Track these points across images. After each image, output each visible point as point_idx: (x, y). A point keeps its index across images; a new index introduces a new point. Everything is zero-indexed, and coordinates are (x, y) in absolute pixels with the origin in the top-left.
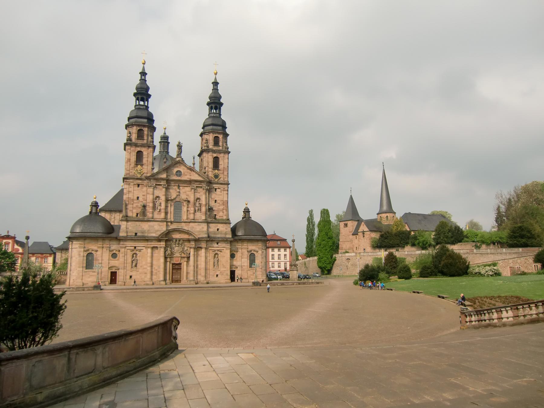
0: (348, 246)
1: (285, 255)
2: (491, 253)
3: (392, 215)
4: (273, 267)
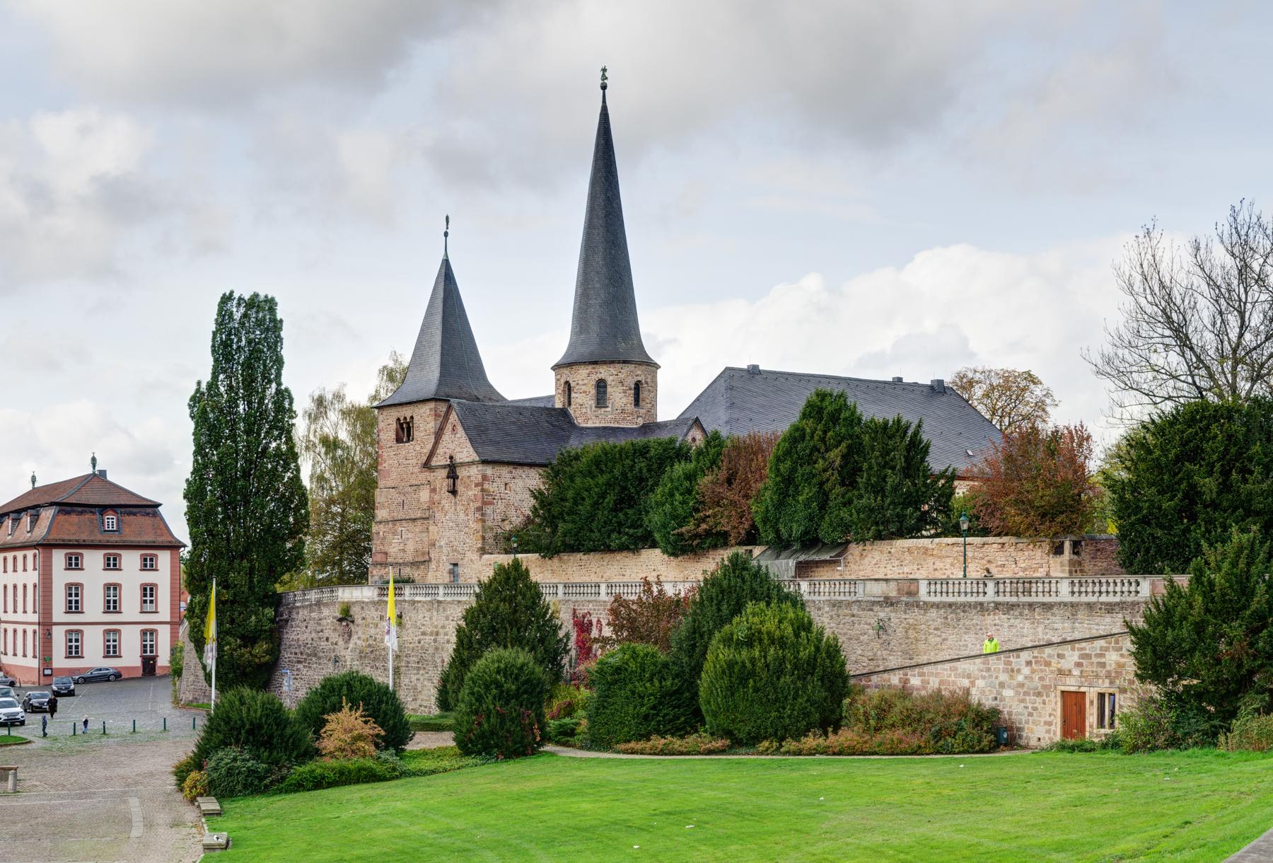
0: (411, 547)
1: (148, 591)
2: (997, 605)
3: (629, 375)
4: (74, 651)
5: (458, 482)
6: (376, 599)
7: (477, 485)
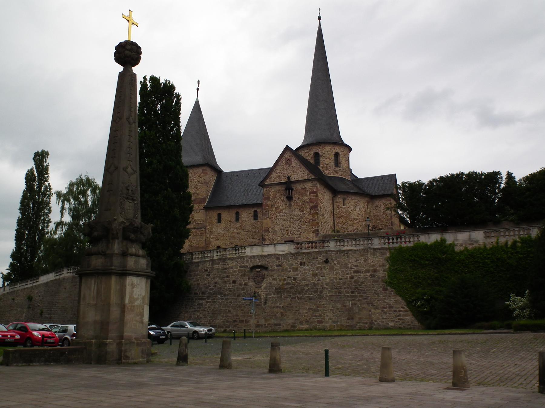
5: (293, 192)
6: (293, 251)
7: (311, 193)
